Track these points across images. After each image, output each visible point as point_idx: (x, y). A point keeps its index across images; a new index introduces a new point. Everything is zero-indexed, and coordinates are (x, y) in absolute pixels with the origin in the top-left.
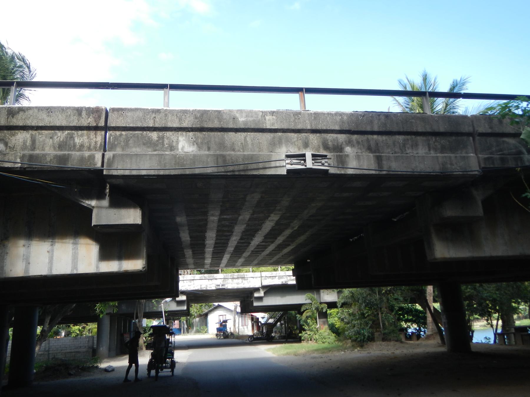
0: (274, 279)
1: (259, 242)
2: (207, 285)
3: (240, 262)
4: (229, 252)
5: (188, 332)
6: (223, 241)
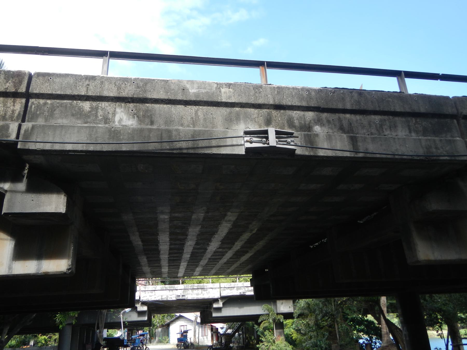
0: (233, 290)
1: (216, 248)
2: (168, 296)
3: (198, 271)
4: (186, 259)
5: (150, 343)
6: (177, 246)
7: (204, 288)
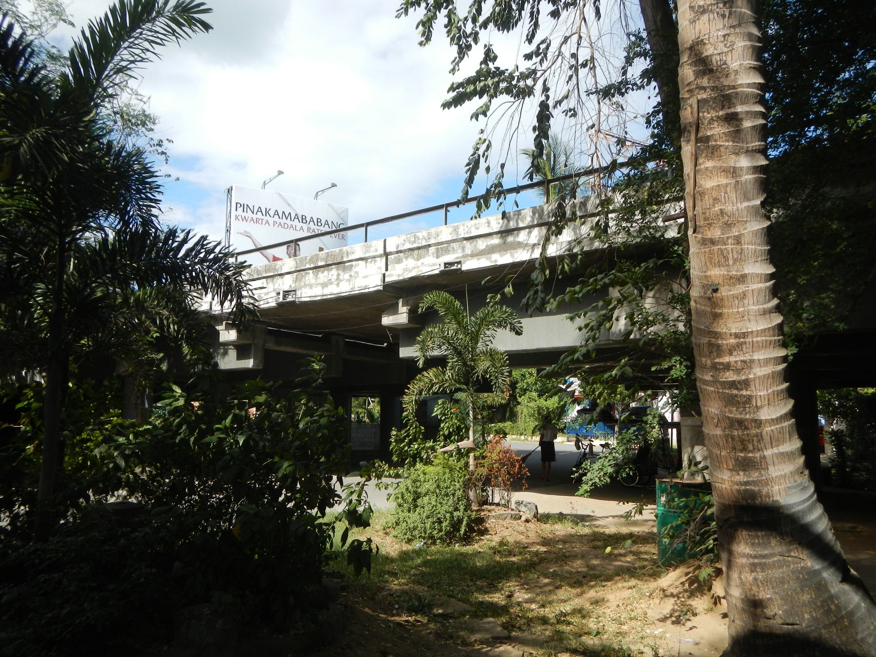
7: (344, 262)
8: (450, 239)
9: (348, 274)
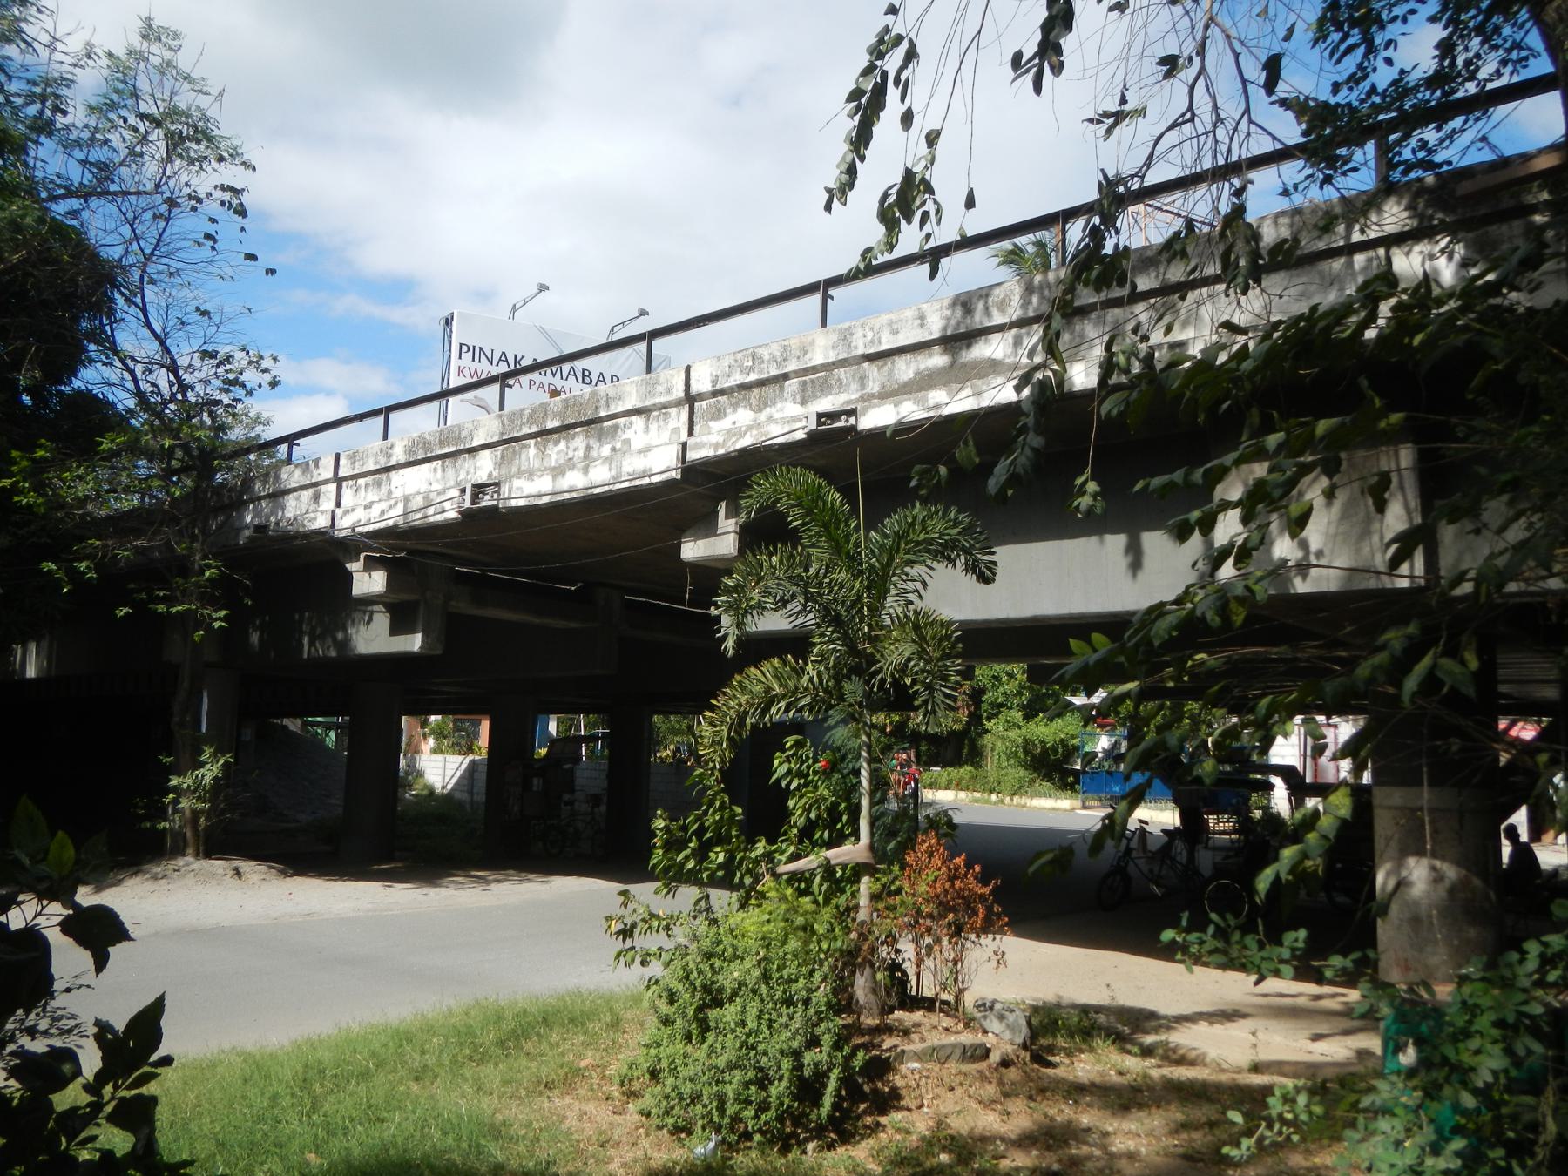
0: (774, 404)
7: (600, 420)
8: (832, 357)
9: (609, 446)
